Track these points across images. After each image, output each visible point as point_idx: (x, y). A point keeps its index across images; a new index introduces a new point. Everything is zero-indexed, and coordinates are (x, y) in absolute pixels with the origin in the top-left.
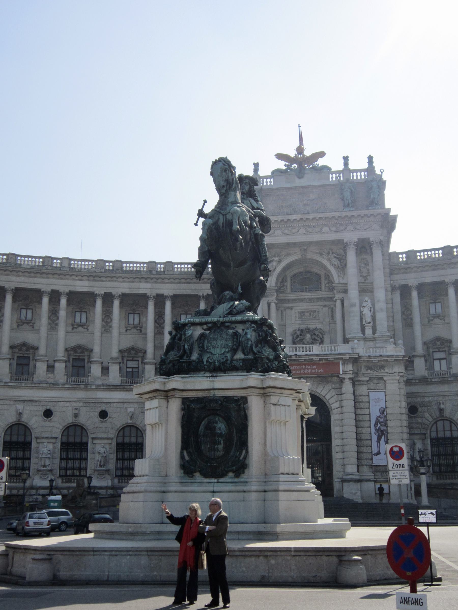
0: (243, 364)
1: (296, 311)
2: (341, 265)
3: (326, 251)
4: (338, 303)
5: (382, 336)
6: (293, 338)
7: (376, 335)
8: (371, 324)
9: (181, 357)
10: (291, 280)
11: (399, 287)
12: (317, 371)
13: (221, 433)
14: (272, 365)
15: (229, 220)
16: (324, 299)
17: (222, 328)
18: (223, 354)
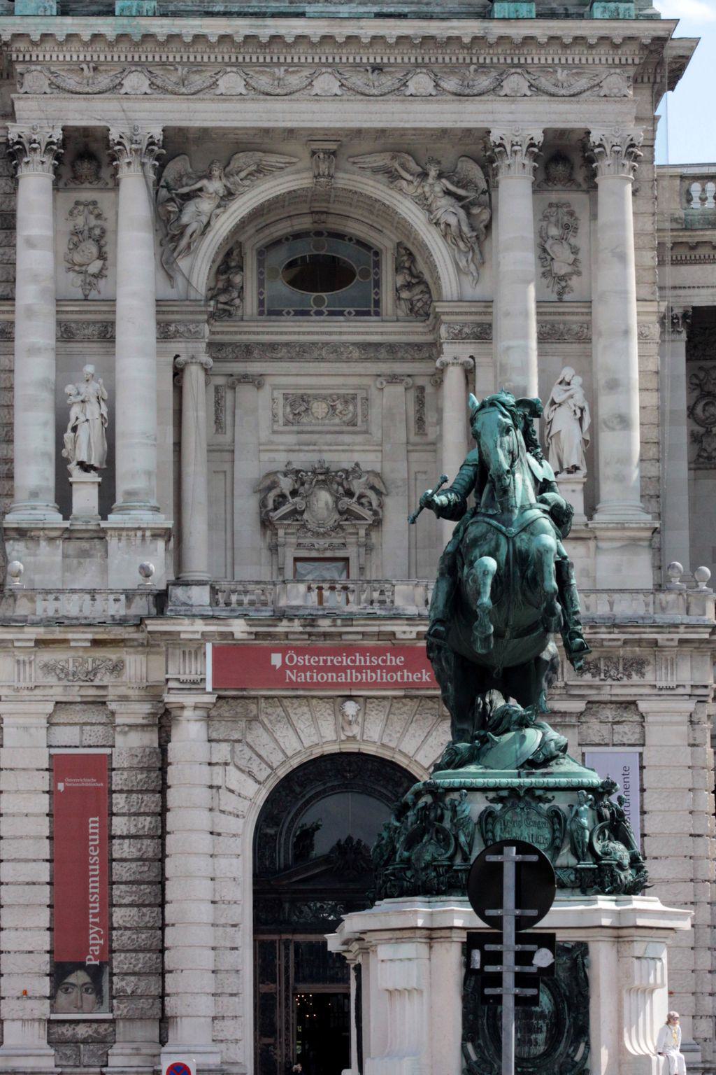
0: (576, 878)
1: (278, 394)
2: (473, 228)
3: (412, 165)
4: (454, 378)
5: (622, 526)
6: (263, 504)
7: (597, 517)
8: (580, 475)
9: (451, 858)
10: (261, 263)
11: (685, 316)
12: (408, 676)
13: (542, 1012)
14: (626, 878)
15: (520, 551)
16: (392, 350)
17: (527, 798)
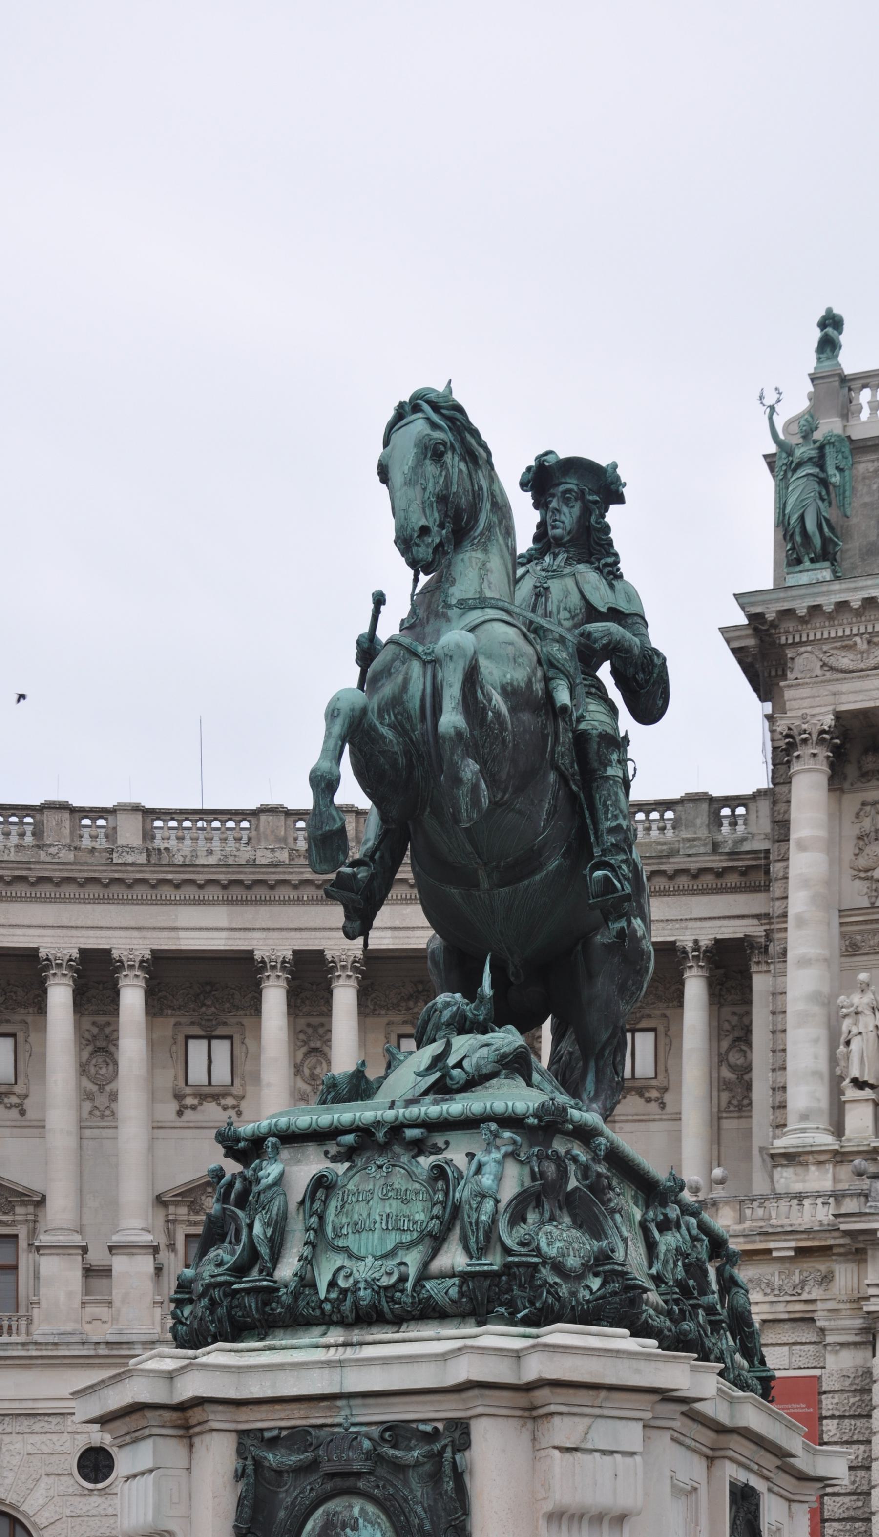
18: (391, 1254)
